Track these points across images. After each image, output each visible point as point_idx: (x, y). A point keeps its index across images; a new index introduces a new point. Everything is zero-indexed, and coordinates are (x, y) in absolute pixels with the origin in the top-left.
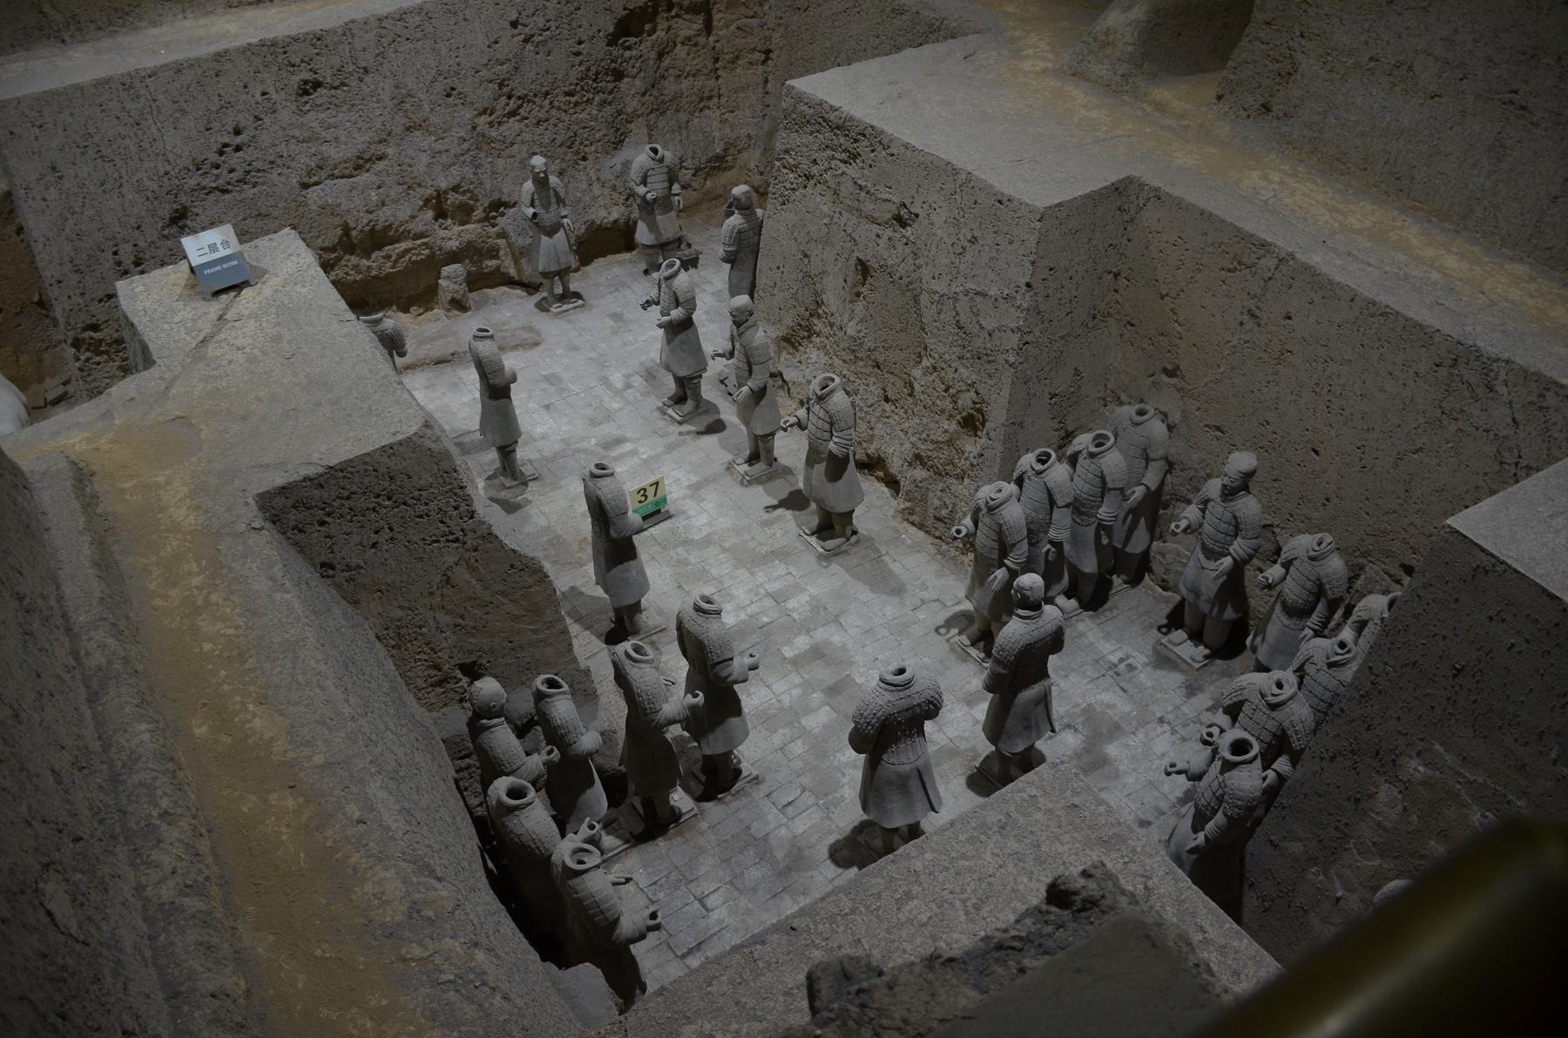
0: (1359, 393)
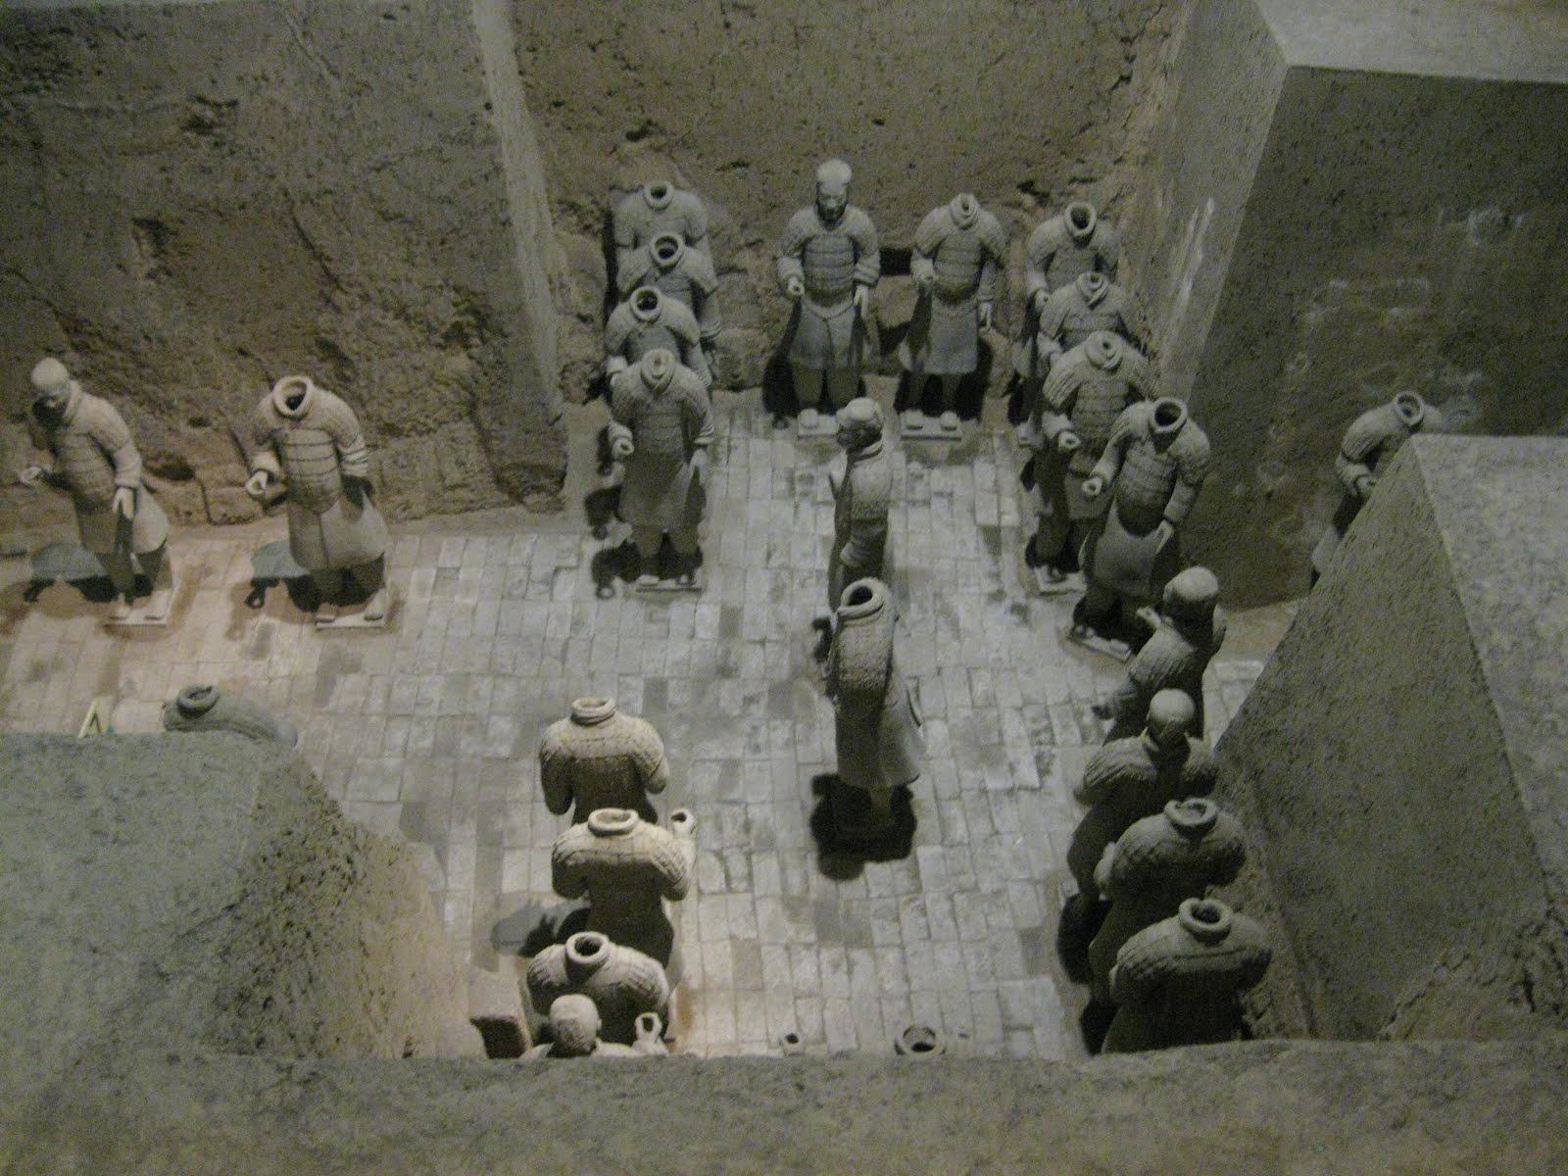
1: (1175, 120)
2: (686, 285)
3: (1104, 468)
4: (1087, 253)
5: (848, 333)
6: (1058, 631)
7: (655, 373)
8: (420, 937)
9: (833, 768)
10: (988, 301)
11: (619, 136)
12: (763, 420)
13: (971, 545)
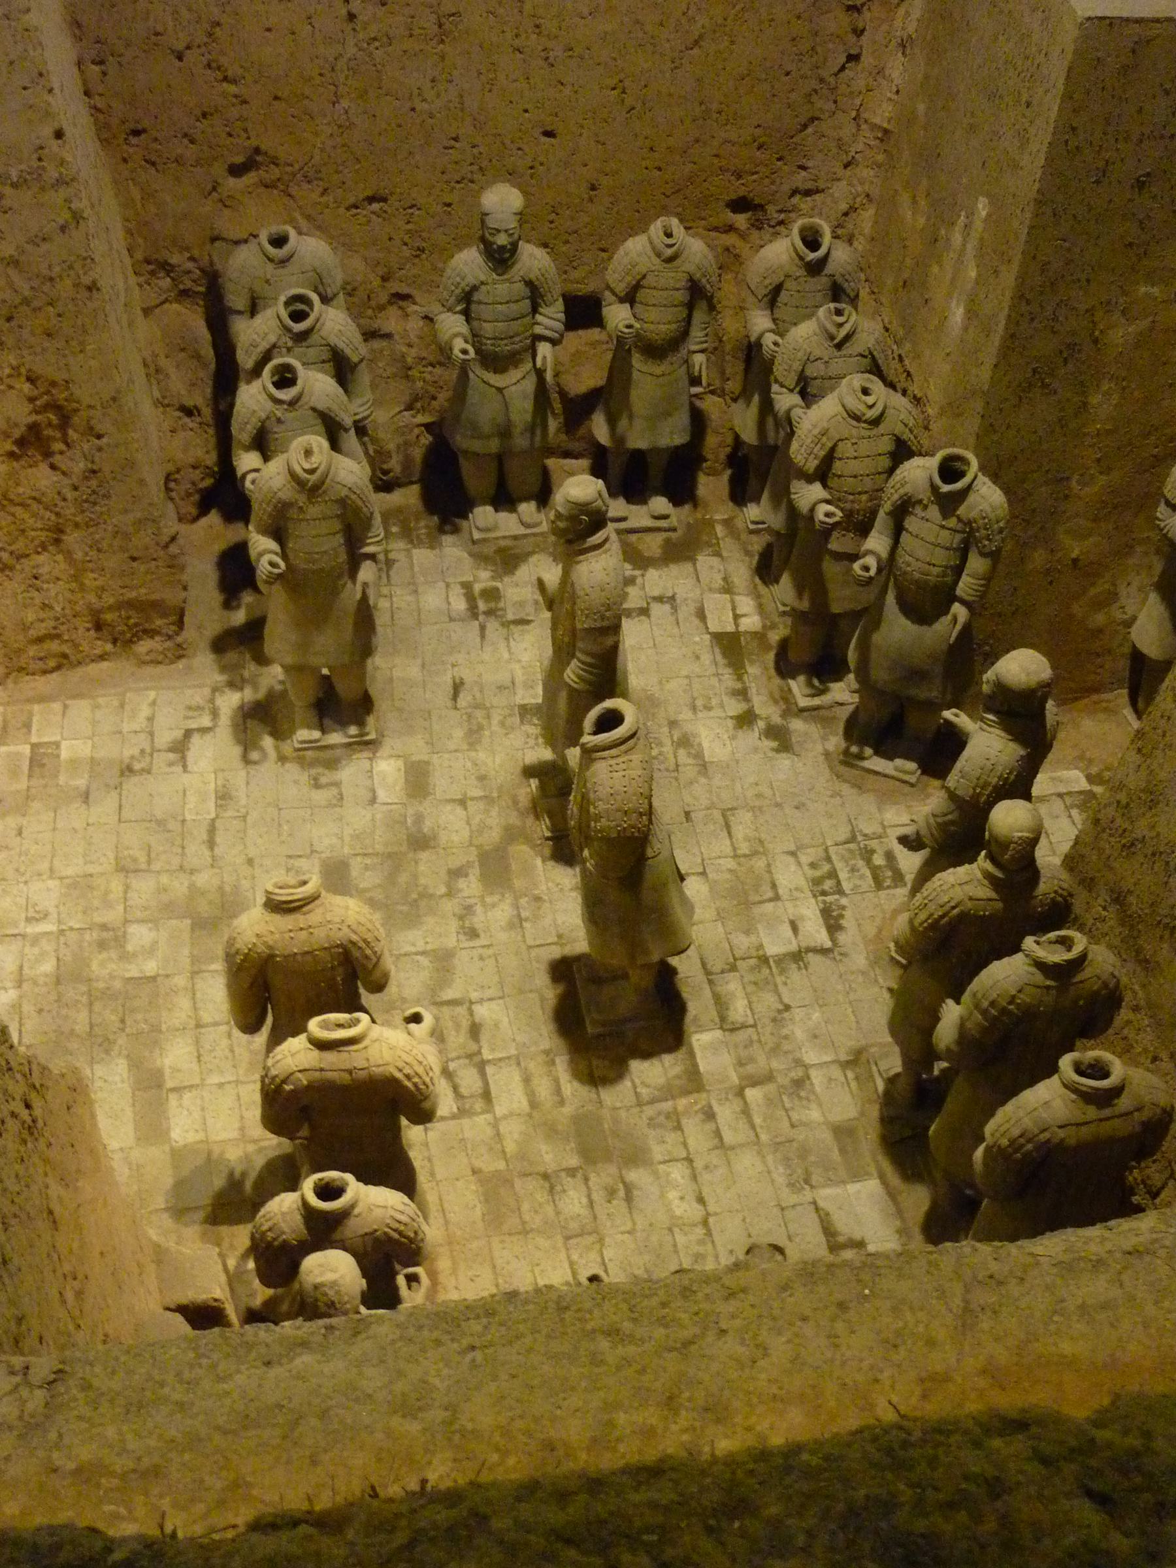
0: (586, 11)
1: (921, 108)
2: (326, 355)
3: (877, 542)
4: (822, 281)
5: (529, 405)
6: (827, 754)
7: (307, 466)
8: (105, 1204)
9: (580, 943)
10: (702, 351)
11: (219, 169)
12: (426, 523)
13: (706, 658)
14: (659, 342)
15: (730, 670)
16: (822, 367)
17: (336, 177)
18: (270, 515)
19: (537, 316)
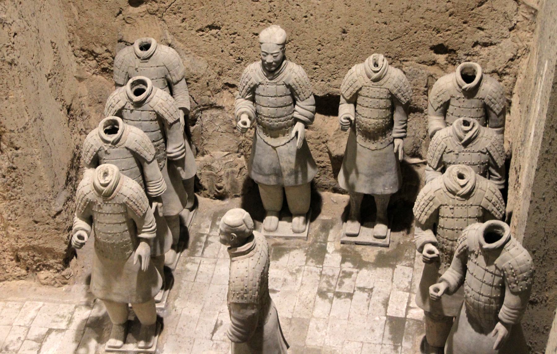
5: (293, 159)
7: (103, 182)
10: (402, 138)
13: (378, 332)
14: (371, 129)
15: (391, 343)
16: (455, 156)
17: (189, 12)
18: (82, 208)
19: (296, 106)
